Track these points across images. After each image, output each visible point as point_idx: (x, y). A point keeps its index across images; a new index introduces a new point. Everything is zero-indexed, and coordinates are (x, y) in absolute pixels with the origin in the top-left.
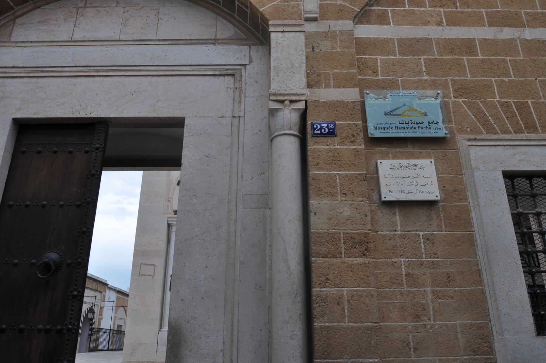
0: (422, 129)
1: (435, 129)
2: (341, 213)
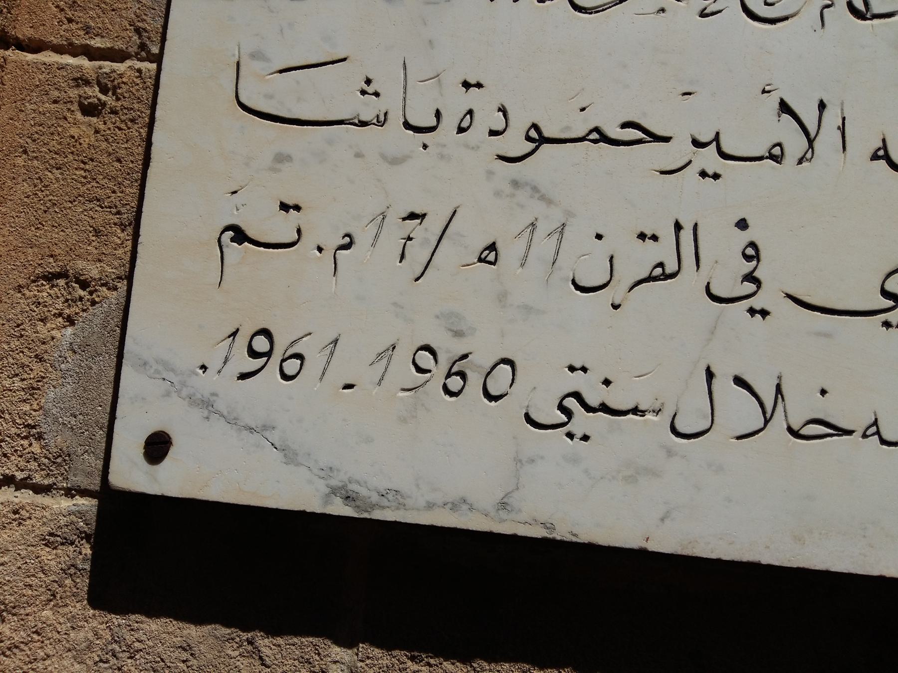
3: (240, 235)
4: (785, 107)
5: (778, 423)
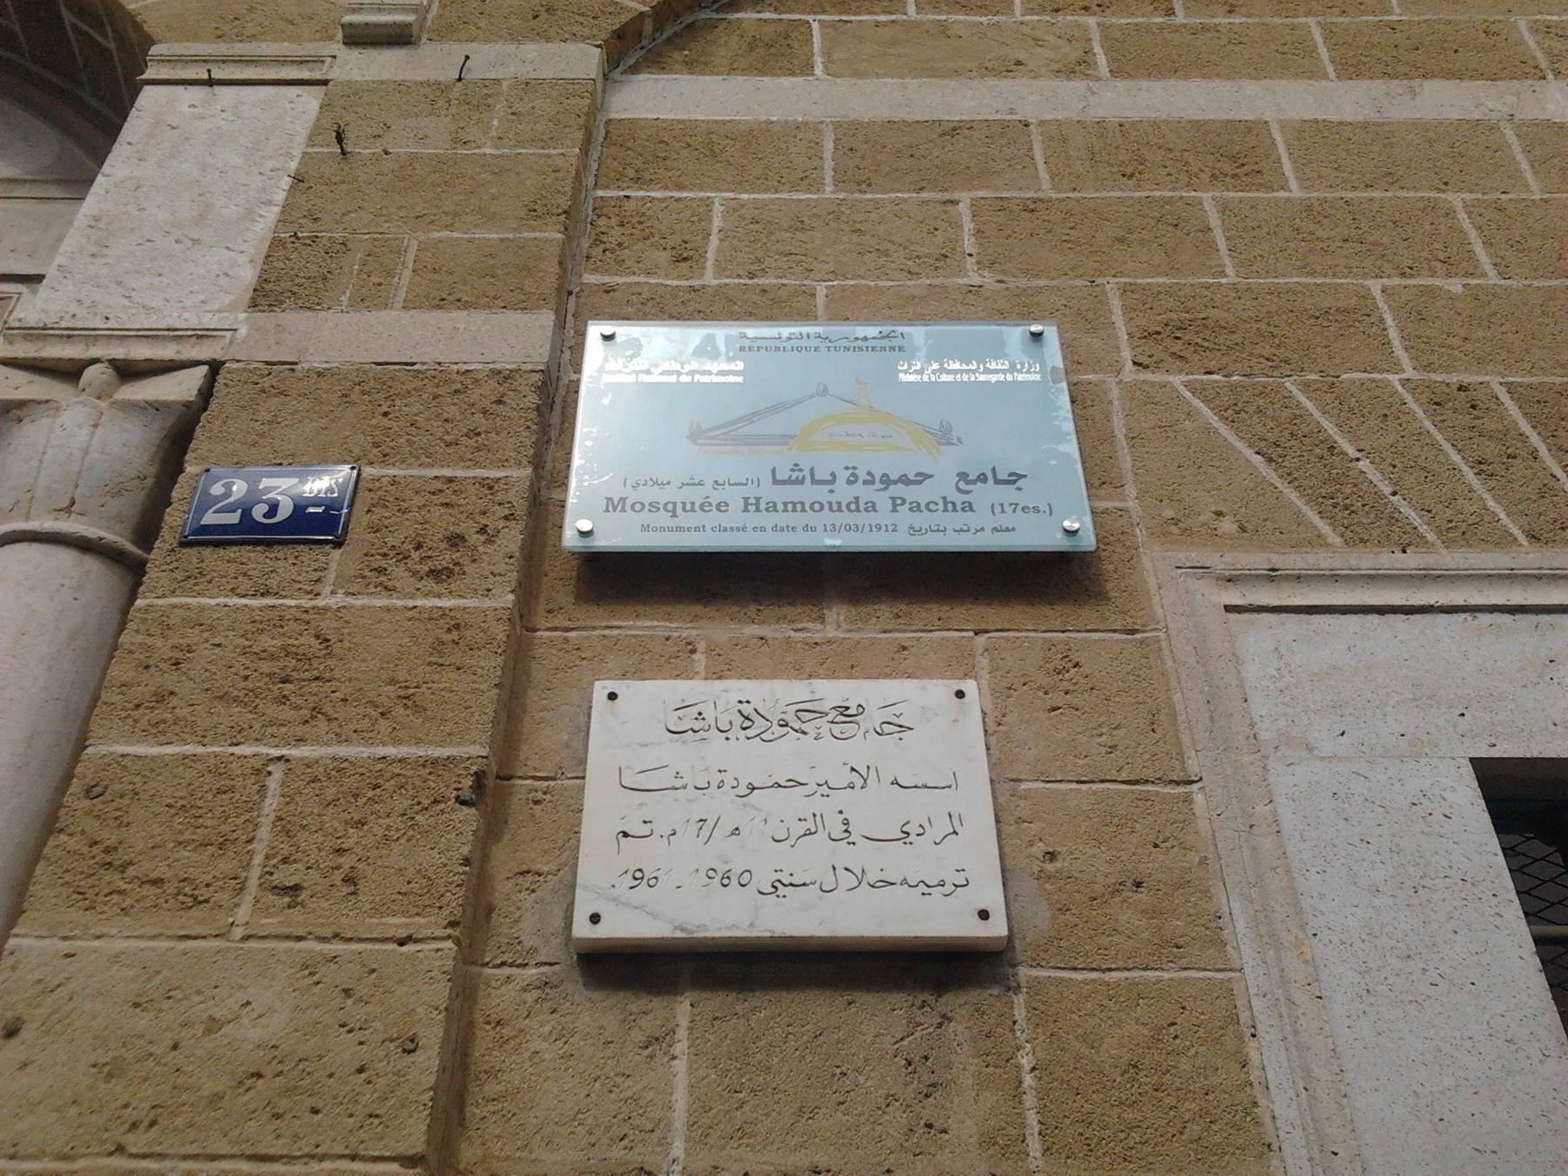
0: (916, 507)
1: (997, 508)
2: (213, 1025)
3: (625, 835)
4: (853, 769)
5: (864, 882)
